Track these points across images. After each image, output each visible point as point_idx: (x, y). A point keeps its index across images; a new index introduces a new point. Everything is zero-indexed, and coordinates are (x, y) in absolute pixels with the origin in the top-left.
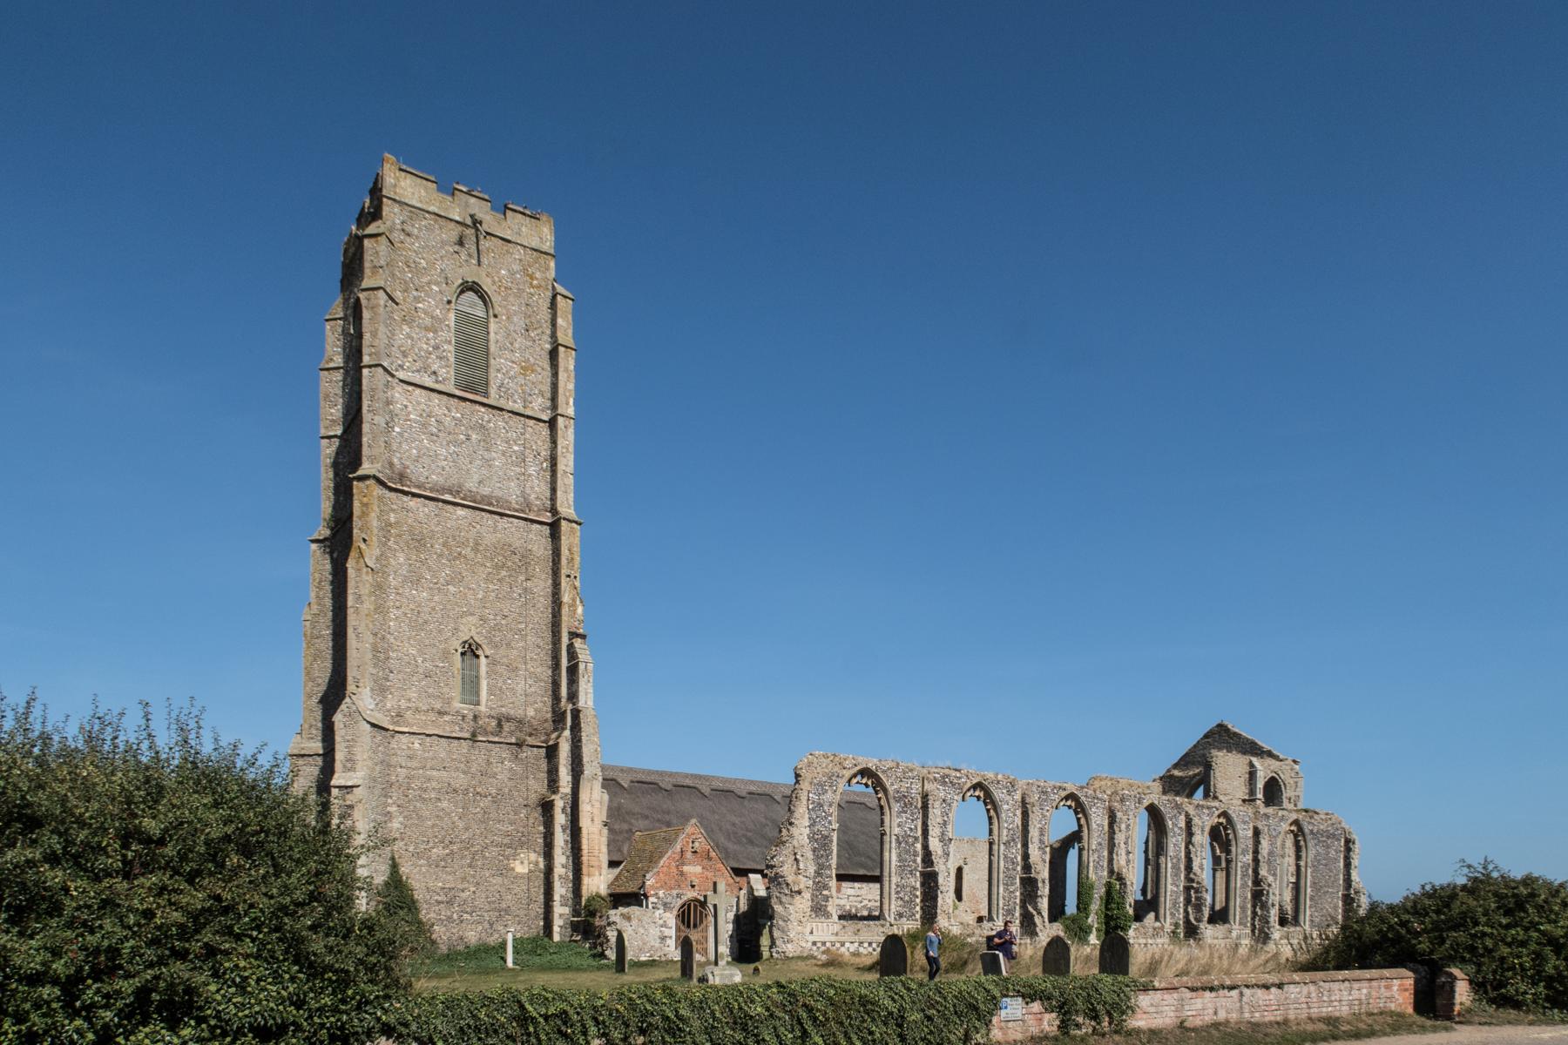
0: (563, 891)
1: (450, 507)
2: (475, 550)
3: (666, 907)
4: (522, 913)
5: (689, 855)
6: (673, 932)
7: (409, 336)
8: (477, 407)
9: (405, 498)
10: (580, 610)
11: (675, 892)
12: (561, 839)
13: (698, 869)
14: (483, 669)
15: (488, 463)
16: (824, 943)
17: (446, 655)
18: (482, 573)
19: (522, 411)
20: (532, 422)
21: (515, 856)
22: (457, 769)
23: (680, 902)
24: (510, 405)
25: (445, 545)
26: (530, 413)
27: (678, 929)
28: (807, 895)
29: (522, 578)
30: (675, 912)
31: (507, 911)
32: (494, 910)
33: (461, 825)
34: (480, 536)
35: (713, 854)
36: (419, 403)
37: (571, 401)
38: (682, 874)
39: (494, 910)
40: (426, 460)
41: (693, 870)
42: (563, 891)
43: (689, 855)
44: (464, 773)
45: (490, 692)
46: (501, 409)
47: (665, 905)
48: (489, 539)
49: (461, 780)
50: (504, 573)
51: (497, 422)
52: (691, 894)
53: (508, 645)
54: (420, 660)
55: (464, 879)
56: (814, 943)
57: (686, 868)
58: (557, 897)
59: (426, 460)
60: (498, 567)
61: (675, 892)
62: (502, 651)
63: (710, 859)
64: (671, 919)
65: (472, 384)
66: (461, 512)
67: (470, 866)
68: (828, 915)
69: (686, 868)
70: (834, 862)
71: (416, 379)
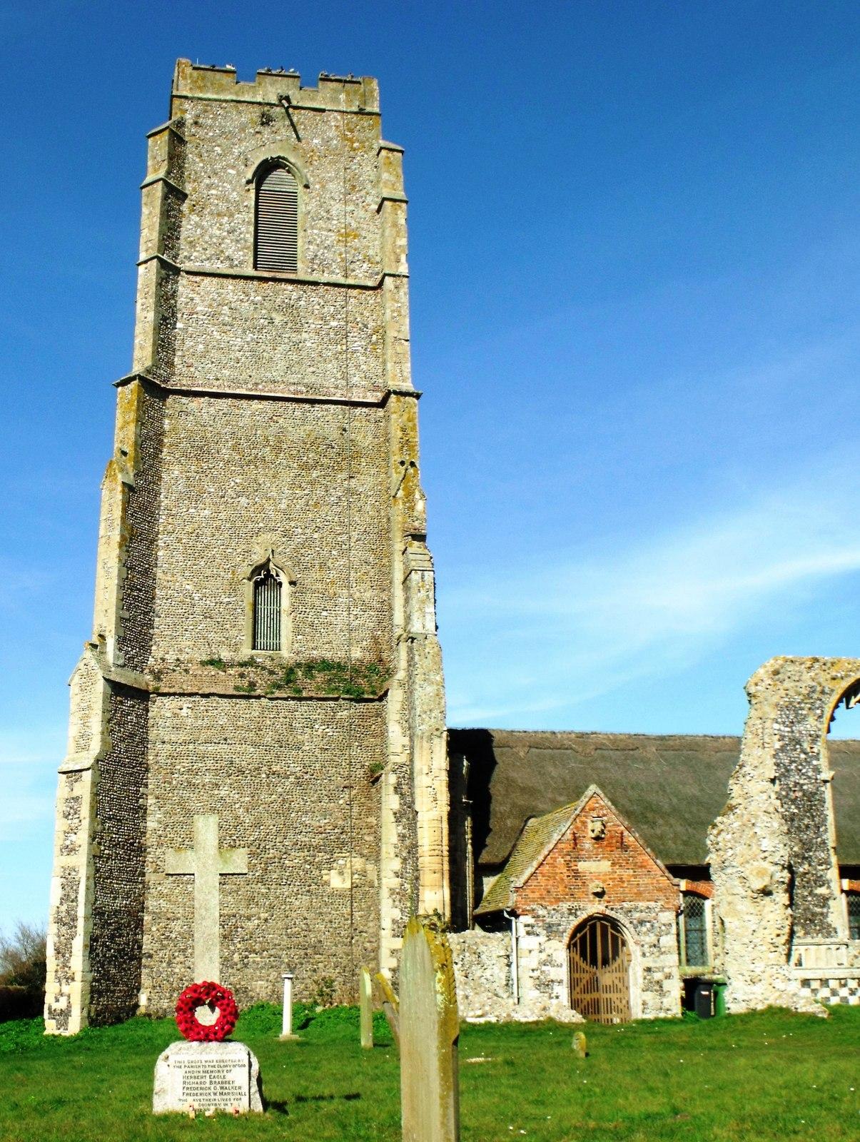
0: (397, 914)
1: (244, 403)
2: (278, 449)
3: (551, 930)
4: (340, 950)
5: (588, 844)
6: (562, 973)
7: (197, 225)
8: (283, 286)
9: (184, 400)
10: (420, 506)
11: (564, 906)
12: (391, 833)
13: (605, 866)
14: (286, 602)
15: (297, 346)
16: (825, 982)
17: (233, 588)
18: (287, 477)
19: (342, 281)
20: (355, 292)
21: (330, 863)
22: (244, 741)
23: (575, 922)
24: (325, 278)
25: (234, 448)
26: (350, 281)
27: (573, 967)
28: (783, 898)
29: (344, 475)
30: (566, 939)
31: (317, 948)
32: (297, 946)
33: (248, 820)
34: (282, 430)
35: (630, 839)
36: (208, 293)
37: (403, 258)
38: (577, 875)
39: (297, 946)
40: (214, 354)
41: (596, 868)
42: (397, 914)
43: (588, 844)
44: (254, 744)
45: (297, 631)
46: (316, 284)
47: (549, 927)
48: (296, 434)
49: (247, 755)
50: (315, 474)
51: (313, 298)
52: (596, 907)
53: (323, 566)
54: (196, 596)
55: (251, 900)
56: (806, 983)
57: (582, 866)
58: (386, 923)
59: (214, 354)
60: (305, 467)
61: (564, 906)
62: (315, 574)
63: (623, 847)
64: (559, 951)
65: (272, 257)
66: (256, 405)
67: (261, 880)
68: (828, 931)
69: (582, 866)
70: (830, 837)
71: (207, 267)
